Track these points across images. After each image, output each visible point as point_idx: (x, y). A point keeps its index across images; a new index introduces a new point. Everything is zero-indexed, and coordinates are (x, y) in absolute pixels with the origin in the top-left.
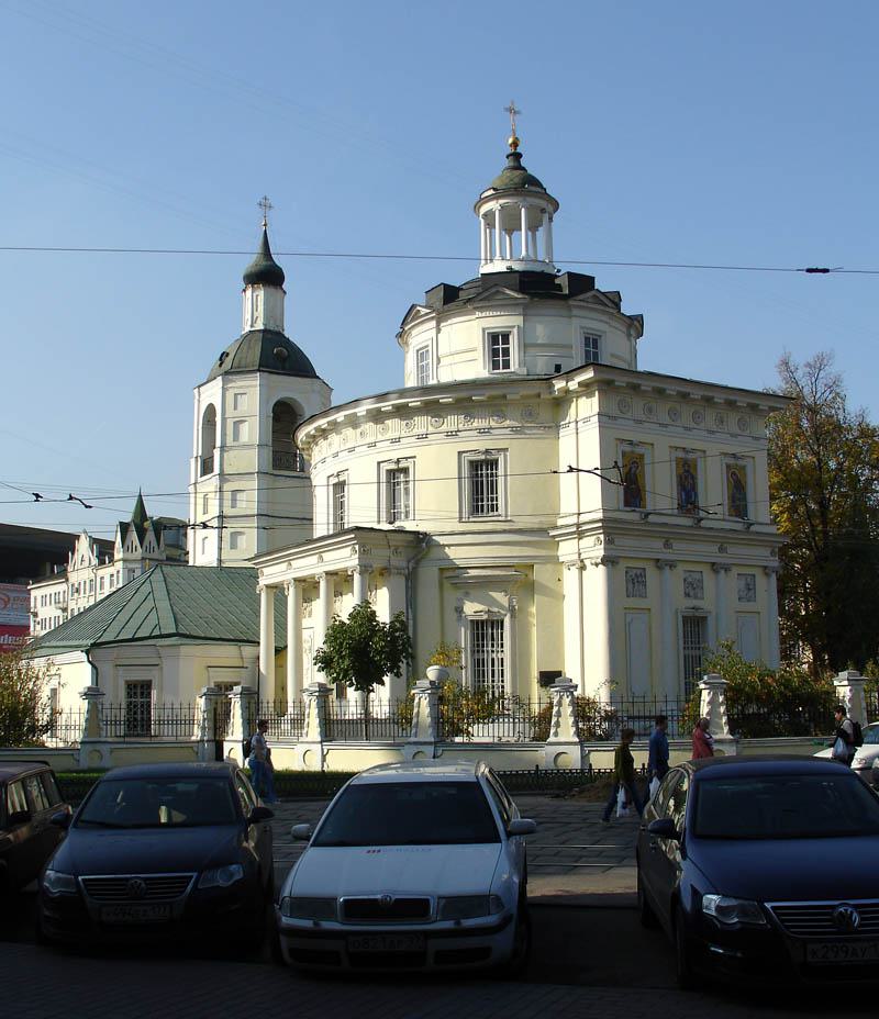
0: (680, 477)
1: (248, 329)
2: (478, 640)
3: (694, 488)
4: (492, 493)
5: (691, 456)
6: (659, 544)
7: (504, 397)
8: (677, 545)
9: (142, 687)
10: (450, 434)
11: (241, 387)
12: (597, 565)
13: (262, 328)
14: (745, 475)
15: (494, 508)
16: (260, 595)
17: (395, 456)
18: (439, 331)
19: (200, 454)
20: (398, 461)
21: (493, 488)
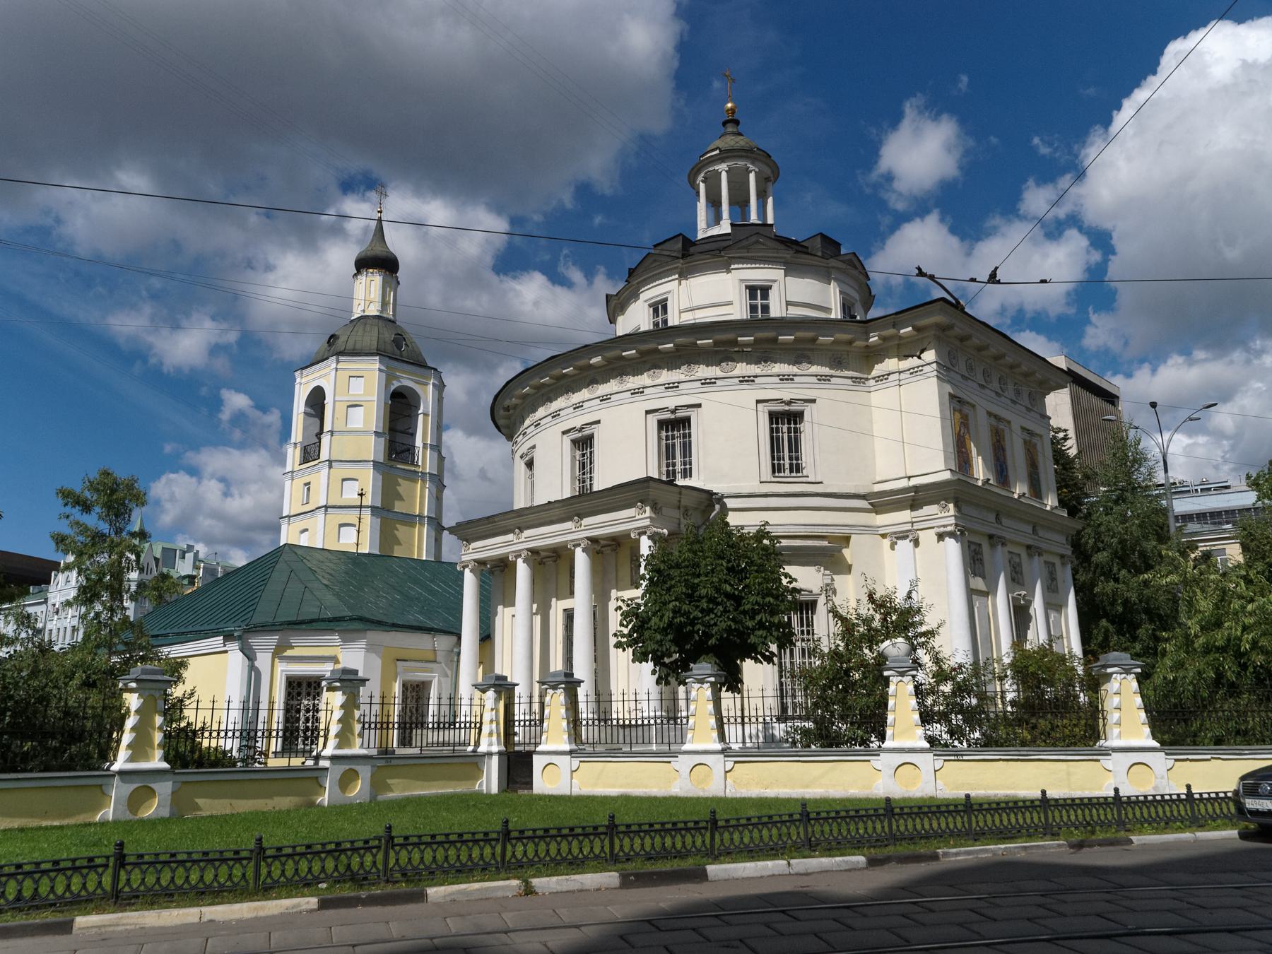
0: (994, 445)
1: (357, 314)
2: (802, 626)
3: (1005, 462)
4: (778, 451)
5: (1001, 426)
6: (992, 518)
7: (814, 340)
8: (1005, 521)
9: (309, 685)
10: (746, 380)
11: (357, 370)
12: (941, 537)
13: (378, 314)
14: (1037, 455)
15: (796, 468)
16: (462, 573)
17: (671, 403)
18: (680, 284)
19: (300, 439)
20: (674, 411)
21: (795, 445)
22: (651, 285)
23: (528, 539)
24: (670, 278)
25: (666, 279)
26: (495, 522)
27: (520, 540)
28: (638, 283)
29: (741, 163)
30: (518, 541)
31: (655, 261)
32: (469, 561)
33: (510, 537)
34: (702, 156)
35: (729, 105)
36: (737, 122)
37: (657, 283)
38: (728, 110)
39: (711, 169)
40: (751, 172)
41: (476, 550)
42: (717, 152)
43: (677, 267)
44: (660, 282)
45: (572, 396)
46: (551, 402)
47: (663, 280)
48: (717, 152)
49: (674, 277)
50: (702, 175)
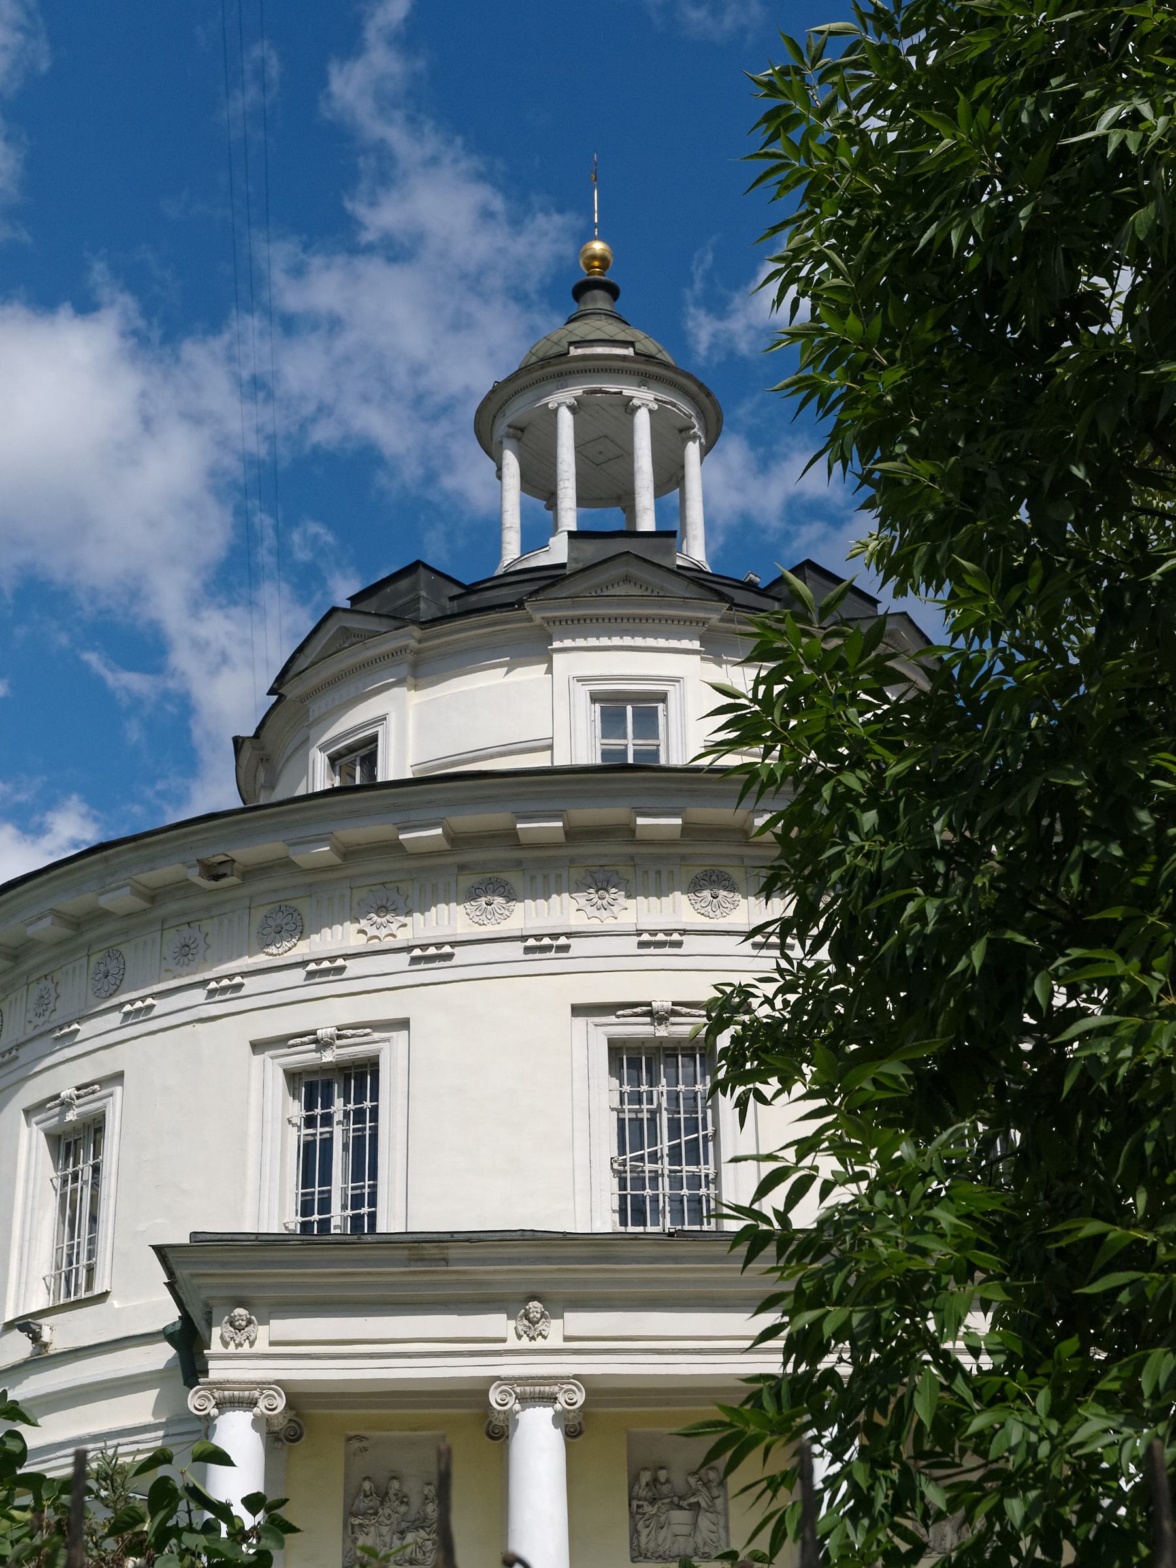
22: (616, 641)
23: (575, 1345)
24: (674, 643)
25: (662, 643)
26: (446, 1261)
27: (539, 1343)
28: (548, 620)
29: (686, 408)
30: (525, 1343)
31: (627, 579)
32: (262, 1385)
33: (496, 1324)
34: (578, 344)
35: (598, 247)
36: (613, 291)
37: (627, 641)
38: (594, 257)
39: (613, 388)
40: (694, 438)
41: (284, 1349)
42: (630, 352)
43: (704, 622)
44: (639, 641)
45: (622, 900)
46: (511, 897)
47: (650, 642)
48: (630, 352)
49: (686, 644)
50: (578, 391)
